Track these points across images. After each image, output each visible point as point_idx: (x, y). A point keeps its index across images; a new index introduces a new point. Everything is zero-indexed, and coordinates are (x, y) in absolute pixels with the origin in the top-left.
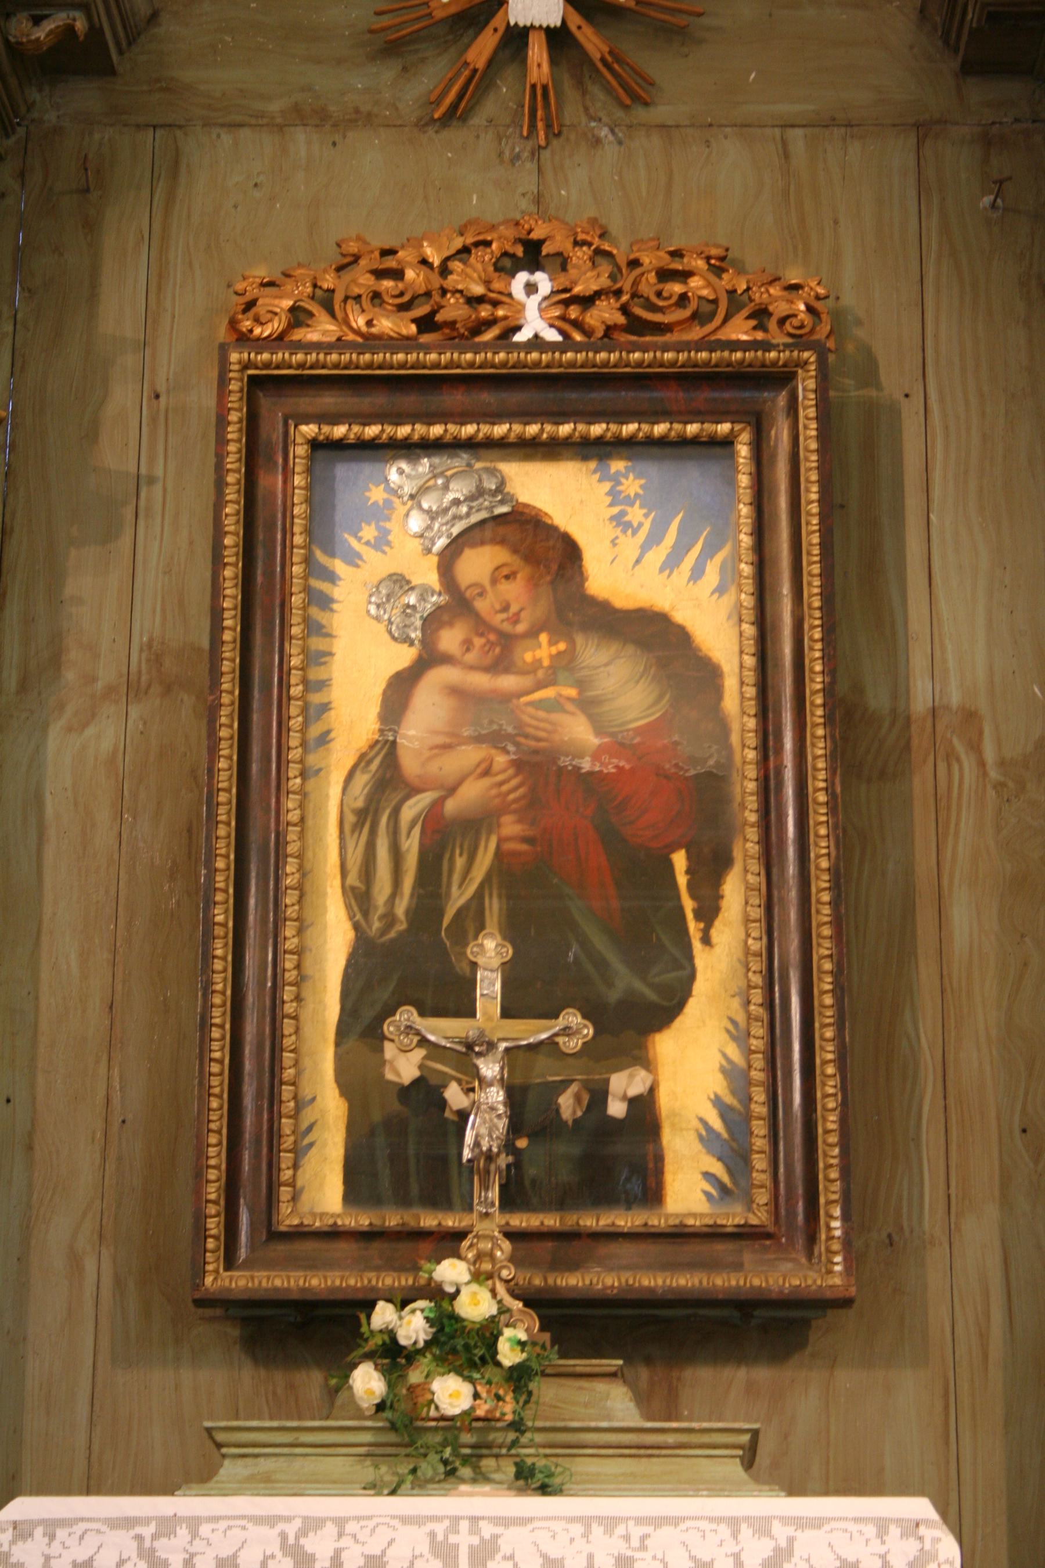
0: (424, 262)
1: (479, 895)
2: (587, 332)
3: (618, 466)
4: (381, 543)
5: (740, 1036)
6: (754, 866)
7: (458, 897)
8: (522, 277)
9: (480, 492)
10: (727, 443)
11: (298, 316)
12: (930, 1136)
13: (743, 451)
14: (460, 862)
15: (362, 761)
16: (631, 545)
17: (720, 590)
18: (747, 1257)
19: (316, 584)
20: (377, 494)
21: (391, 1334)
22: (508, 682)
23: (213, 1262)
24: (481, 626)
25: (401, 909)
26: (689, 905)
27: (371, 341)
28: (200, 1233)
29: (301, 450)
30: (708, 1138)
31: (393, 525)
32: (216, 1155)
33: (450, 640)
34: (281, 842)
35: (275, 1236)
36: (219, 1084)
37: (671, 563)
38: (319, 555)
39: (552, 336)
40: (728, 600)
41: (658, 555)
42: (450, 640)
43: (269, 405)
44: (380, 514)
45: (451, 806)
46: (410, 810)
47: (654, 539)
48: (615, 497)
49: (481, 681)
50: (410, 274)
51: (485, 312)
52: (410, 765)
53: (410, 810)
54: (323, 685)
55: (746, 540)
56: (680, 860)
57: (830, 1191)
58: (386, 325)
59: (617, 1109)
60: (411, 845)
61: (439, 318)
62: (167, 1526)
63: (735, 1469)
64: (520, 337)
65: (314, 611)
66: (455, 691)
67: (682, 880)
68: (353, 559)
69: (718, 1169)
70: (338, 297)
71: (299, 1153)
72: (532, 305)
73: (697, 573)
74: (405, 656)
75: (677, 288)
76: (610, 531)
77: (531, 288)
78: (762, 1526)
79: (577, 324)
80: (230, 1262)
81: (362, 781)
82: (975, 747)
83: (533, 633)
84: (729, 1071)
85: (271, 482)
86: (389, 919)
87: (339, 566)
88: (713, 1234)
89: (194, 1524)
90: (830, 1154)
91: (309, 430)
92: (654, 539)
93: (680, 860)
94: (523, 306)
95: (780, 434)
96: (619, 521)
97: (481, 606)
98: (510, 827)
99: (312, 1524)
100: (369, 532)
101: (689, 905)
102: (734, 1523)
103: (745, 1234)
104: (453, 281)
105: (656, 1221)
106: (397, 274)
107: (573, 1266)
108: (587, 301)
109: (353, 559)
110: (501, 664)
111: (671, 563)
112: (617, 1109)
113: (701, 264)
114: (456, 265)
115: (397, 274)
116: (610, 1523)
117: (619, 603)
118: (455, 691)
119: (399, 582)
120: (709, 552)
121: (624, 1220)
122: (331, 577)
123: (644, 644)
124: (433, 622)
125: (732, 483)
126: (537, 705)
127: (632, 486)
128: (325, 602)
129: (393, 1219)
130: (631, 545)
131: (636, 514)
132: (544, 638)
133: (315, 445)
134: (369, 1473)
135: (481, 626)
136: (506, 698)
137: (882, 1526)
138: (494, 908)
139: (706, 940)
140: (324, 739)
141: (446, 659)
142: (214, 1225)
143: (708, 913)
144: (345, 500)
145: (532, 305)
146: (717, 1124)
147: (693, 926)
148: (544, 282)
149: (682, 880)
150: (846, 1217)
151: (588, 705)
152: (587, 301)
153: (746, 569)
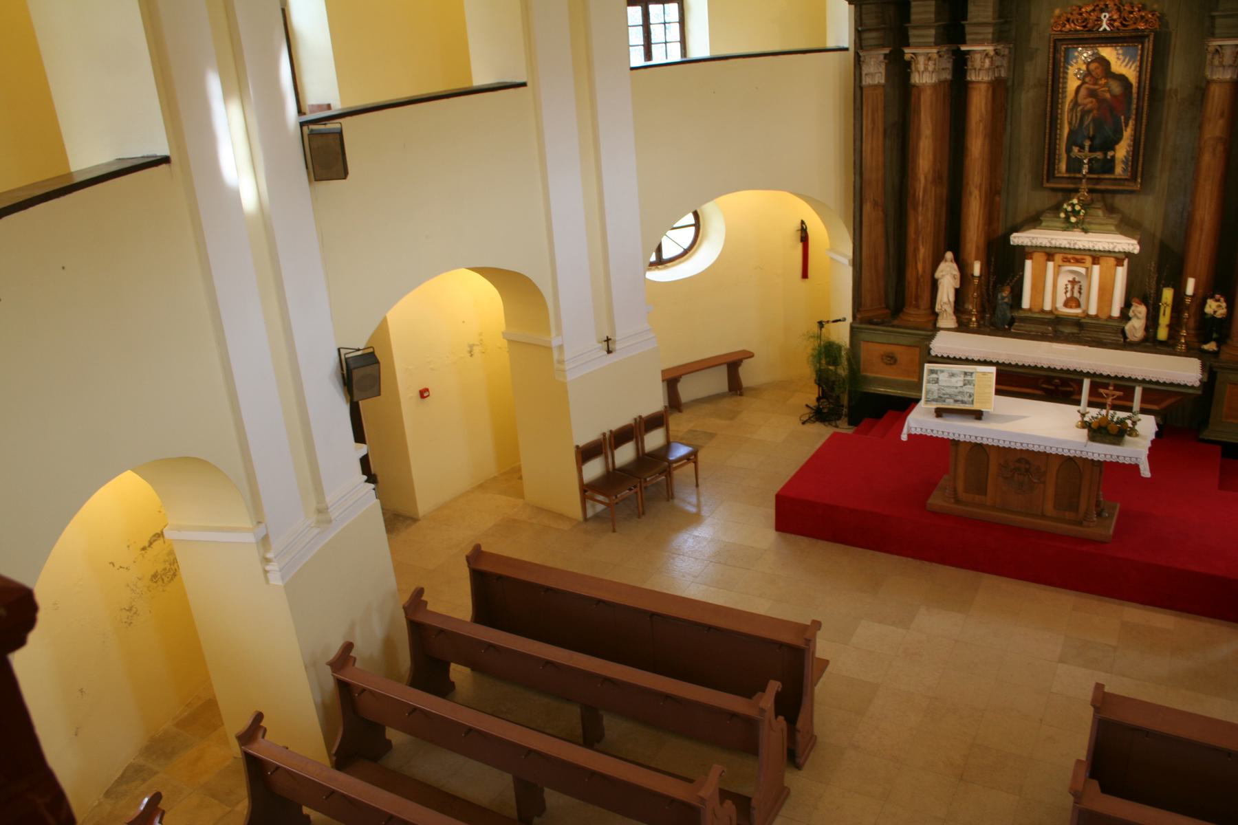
0: (1086, 12)
1: (1089, 124)
2: (1114, 27)
3: (1118, 48)
4: (1077, 63)
5: (1129, 146)
6: (1134, 122)
7: (1086, 123)
8: (1104, 14)
9: (1093, 54)
10: (1137, 46)
11: (1064, 25)
12: (1160, 156)
13: (1140, 46)
14: (1087, 118)
15: (1072, 101)
16: (1119, 62)
17: (1134, 71)
18: (1126, 183)
19: (1066, 70)
20: (1076, 54)
21: (1066, 209)
22: (1096, 87)
23: (1045, 181)
24: (1093, 77)
25: (1077, 125)
26: (1123, 124)
27: (1076, 31)
28: (1043, 179)
29: (1063, 48)
30: (1123, 162)
31: (1079, 60)
32: (1045, 167)
33: (1087, 80)
34: (1057, 116)
35: (1054, 177)
36: (1046, 156)
37: (1126, 65)
38: (1067, 65)
39: (1108, 29)
40: (1135, 73)
41: (1125, 63)
42: (1087, 80)
43: (1059, 44)
44: (1076, 58)
45: (1086, 108)
46: (1079, 108)
47: (1124, 61)
48: (1118, 54)
49: (1092, 87)
50: (1084, 15)
51: (1096, 23)
52: (1080, 101)
53: (1079, 108)
54: (1065, 88)
55: (1138, 63)
56: (1122, 117)
57: (1139, 174)
58: (1078, 28)
59: (1109, 157)
60: (1079, 115)
61: (1089, 25)
62: (1033, 238)
63: (1113, 228)
64: (1101, 29)
65: (1065, 75)
66: (1087, 89)
67: (1123, 121)
68: (1072, 65)
69: (1124, 167)
70: (1071, 21)
71: (1059, 161)
72: (1105, 20)
73: (1130, 67)
74: (1078, 83)
75: (1132, 16)
76: (1116, 60)
77: (1105, 16)
78: (1112, 243)
79: (1112, 25)
80: (1048, 181)
81: (1071, 104)
82: (1176, 96)
83: (1101, 79)
84: (1128, 152)
85: (1058, 56)
86: (1075, 127)
87: (1070, 67)
88: (1121, 179)
89: (1037, 238)
90: (1140, 169)
91: (1065, 46)
92: (1124, 61)
93: (1122, 117)
94: (1102, 21)
95: (1146, 45)
96: (1118, 58)
97: (1093, 73)
98: (1095, 112)
99: (1052, 239)
100: (1075, 61)
101: (1123, 124)
102: (1108, 243)
103: (1126, 179)
104: (1091, 18)
105: (1112, 177)
106: (1081, 14)
107: (1097, 184)
108: (1115, 20)
109: (1072, 65)
110: (1095, 83)
111: (1126, 65)
112: (1109, 157)
113: (1136, 9)
114: (1092, 14)
115: (1081, 14)
116: (1092, 241)
117: (1117, 73)
118: (1087, 89)
119: (1079, 69)
120: (1133, 63)
121: (1107, 176)
122: (1068, 69)
123: (1120, 80)
124: (1085, 76)
125: (1137, 52)
126: (1103, 91)
127: (1120, 52)
128: (1067, 73)
129: (1072, 175)
130: (1119, 62)
131: (1121, 57)
132: (1103, 79)
133: (1065, 48)
134: (1063, 225)
135: (1093, 77)
136: (1095, 90)
137: (1129, 244)
138: (1091, 125)
139: (1126, 130)
140: (1066, 97)
141: (1086, 83)
142: (1045, 177)
143: (1127, 125)
144: (1071, 55)
145: (1105, 20)
146: (1124, 159)
147: (1124, 128)
148: (1108, 15)
149: (1123, 121)
150: (1141, 180)
151: (1109, 91)
152: (1115, 20)
153: (1138, 69)
